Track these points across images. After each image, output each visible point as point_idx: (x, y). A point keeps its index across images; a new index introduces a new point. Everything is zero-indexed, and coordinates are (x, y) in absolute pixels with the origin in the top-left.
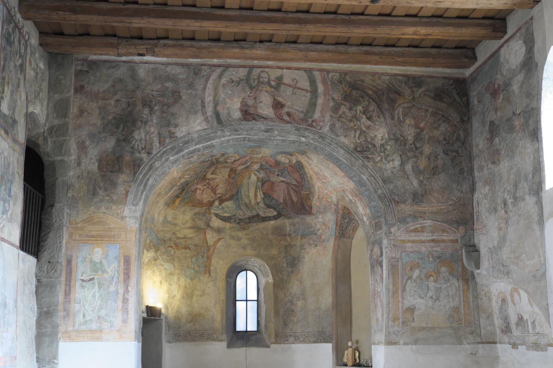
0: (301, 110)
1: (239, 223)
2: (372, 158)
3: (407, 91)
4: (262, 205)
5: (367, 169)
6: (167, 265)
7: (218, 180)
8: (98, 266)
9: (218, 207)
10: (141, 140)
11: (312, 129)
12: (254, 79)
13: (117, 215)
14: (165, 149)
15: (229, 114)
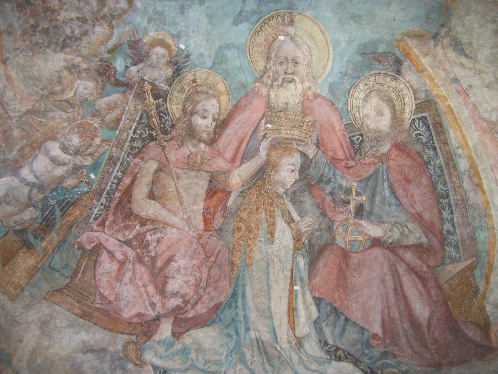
4: (312, 347)
7: (171, 234)
9: (170, 345)
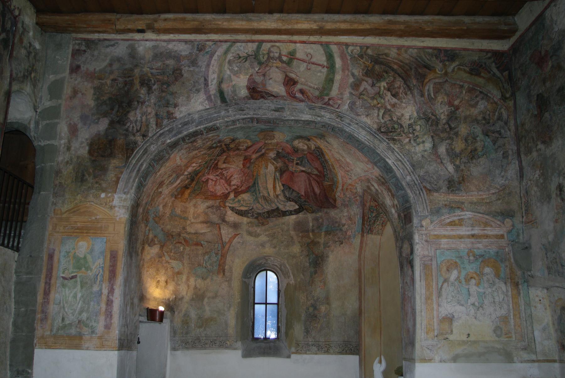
0: (316, 87)
1: (257, 218)
2: (399, 140)
3: (439, 66)
4: (281, 198)
5: (393, 152)
6: (174, 263)
7: (232, 170)
8: (82, 262)
9: (234, 200)
10: (136, 121)
11: (329, 107)
12: (264, 54)
13: (106, 204)
14: (161, 132)
15: (234, 91)
